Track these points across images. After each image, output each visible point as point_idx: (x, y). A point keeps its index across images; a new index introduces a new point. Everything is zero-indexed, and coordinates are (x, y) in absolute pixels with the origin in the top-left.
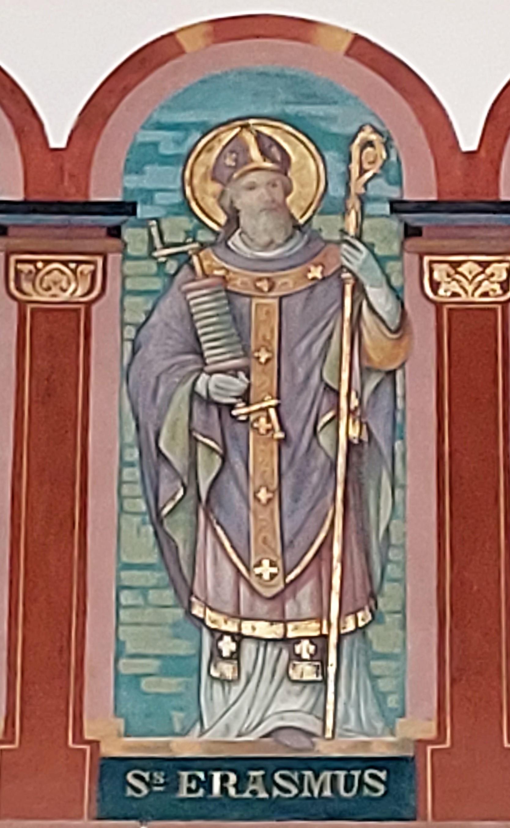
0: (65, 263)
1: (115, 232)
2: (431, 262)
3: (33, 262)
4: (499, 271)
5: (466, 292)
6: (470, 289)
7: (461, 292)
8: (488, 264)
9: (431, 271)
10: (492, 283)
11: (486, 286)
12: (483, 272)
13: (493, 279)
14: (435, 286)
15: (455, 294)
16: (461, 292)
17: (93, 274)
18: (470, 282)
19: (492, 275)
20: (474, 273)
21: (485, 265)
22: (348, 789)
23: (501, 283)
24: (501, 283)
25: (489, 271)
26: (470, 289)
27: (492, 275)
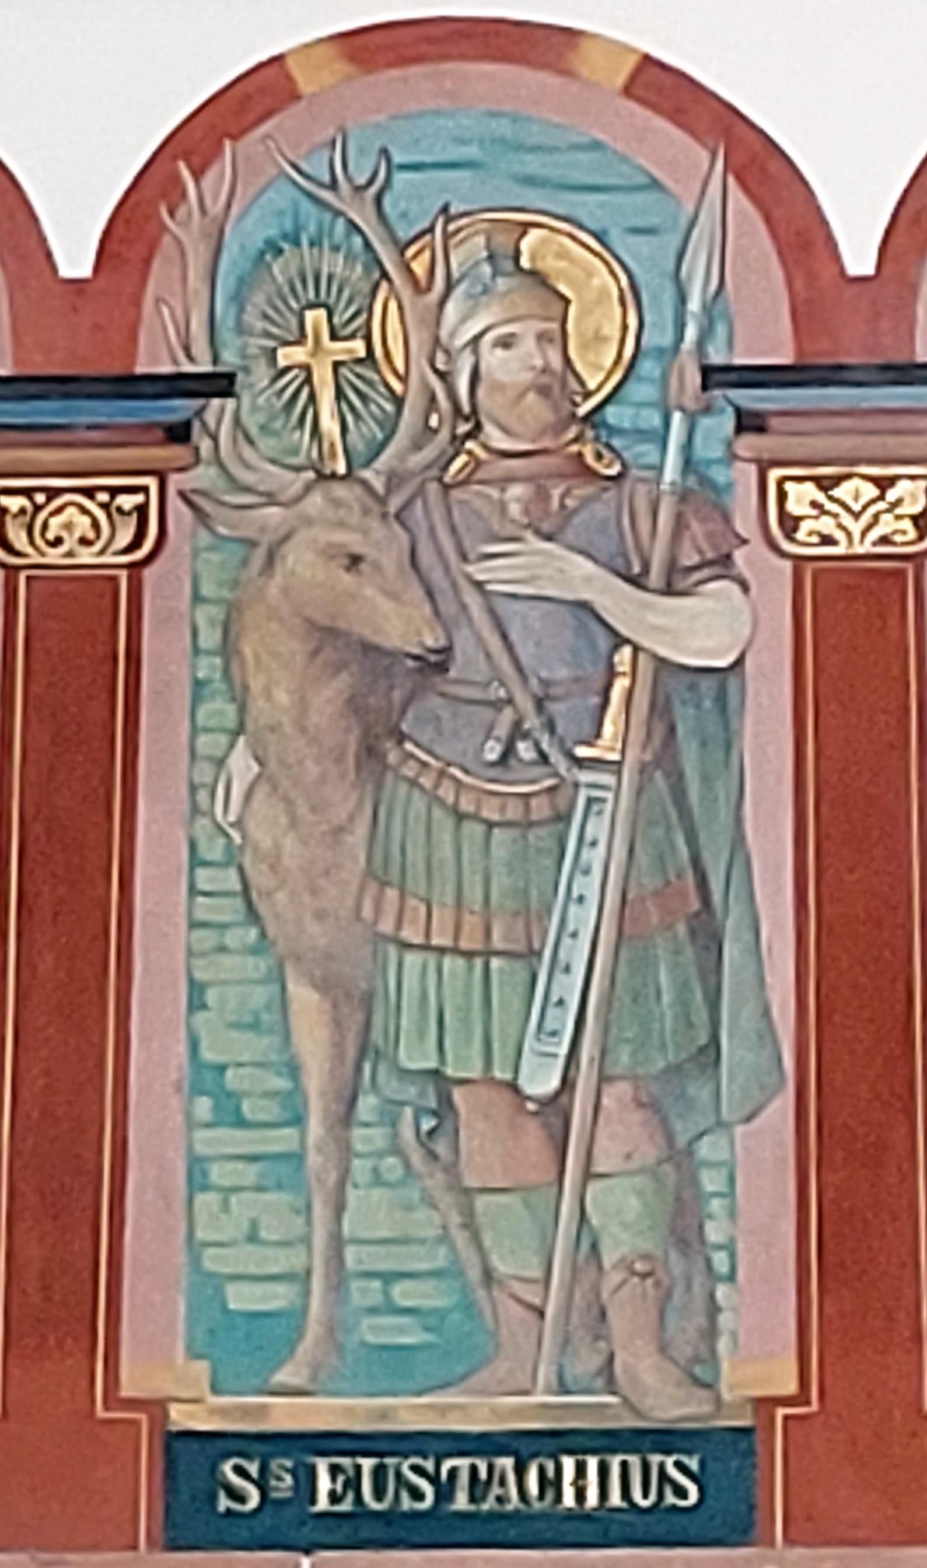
1: (179, 433)
2: (781, 482)
3: (27, 492)
4: (911, 495)
5: (849, 535)
6: (856, 528)
7: (839, 535)
8: (891, 481)
9: (782, 496)
10: (898, 517)
11: (886, 525)
12: (881, 497)
13: (899, 511)
14: (790, 524)
15: (827, 540)
16: (839, 535)
17: (142, 510)
18: (857, 516)
19: (898, 502)
20: (863, 501)
21: (883, 484)
23: (915, 519)
24: (915, 519)
25: (892, 495)
26: (856, 528)
27: (898, 502)
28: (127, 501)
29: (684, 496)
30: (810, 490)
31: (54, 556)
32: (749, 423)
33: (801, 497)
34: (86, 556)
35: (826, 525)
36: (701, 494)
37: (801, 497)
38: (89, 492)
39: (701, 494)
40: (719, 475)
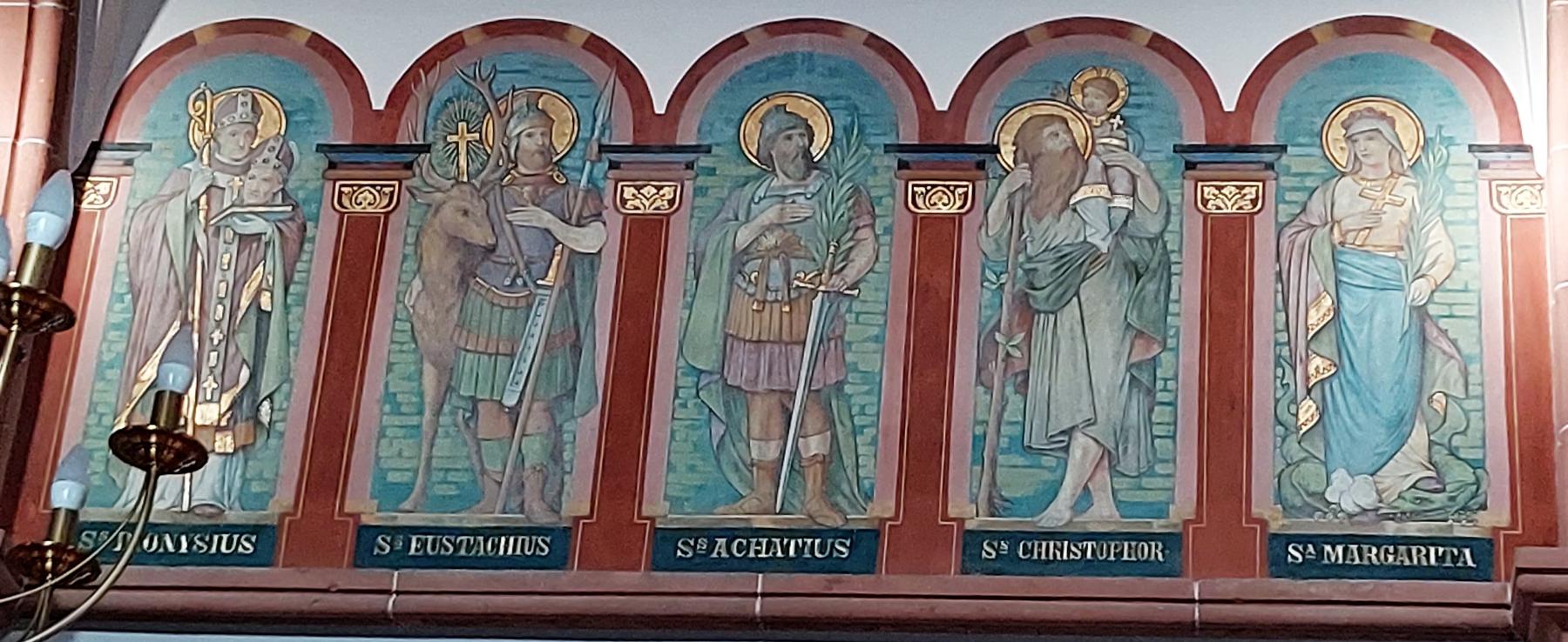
0: (373, 186)
6: (647, 204)
8: (662, 187)
21: (659, 188)
22: (228, 547)
26: (647, 204)
28: (387, 190)
29: (588, 191)
30: (633, 190)
31: (358, 209)
32: (614, 165)
33: (629, 192)
34: (370, 209)
35: (637, 203)
36: (594, 190)
37: (629, 192)
38: (373, 186)
39: (594, 190)
40: (601, 184)
